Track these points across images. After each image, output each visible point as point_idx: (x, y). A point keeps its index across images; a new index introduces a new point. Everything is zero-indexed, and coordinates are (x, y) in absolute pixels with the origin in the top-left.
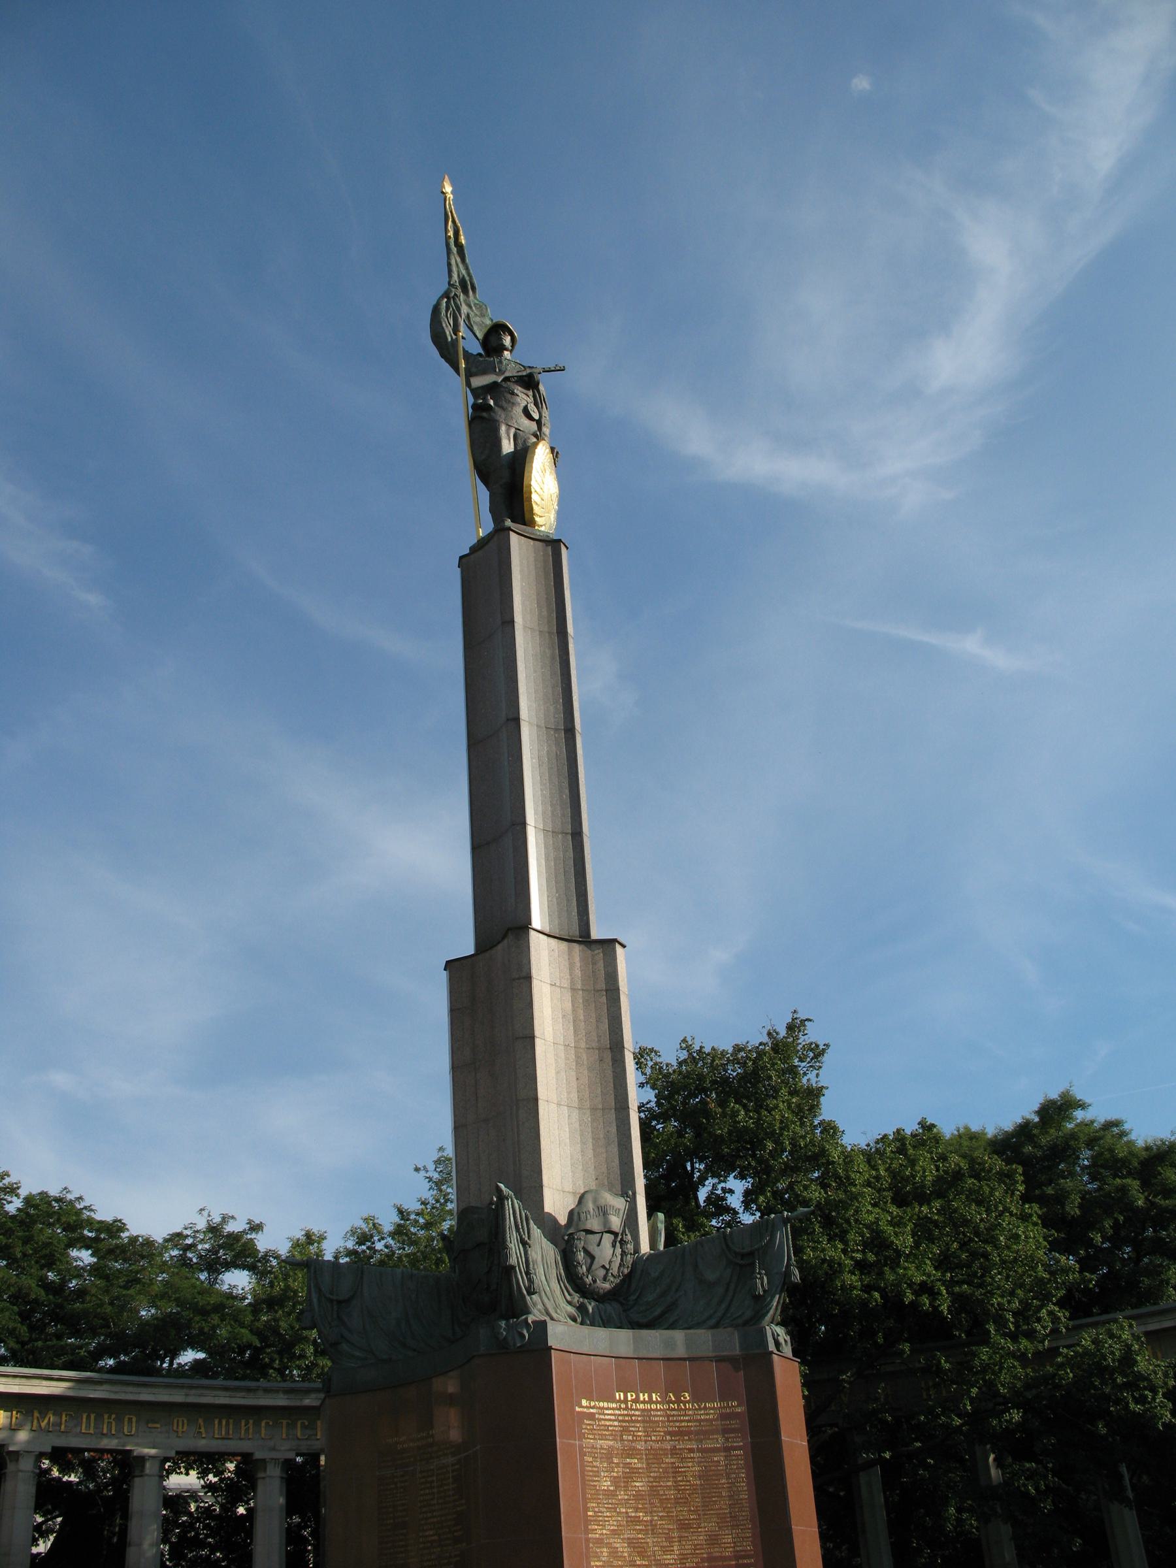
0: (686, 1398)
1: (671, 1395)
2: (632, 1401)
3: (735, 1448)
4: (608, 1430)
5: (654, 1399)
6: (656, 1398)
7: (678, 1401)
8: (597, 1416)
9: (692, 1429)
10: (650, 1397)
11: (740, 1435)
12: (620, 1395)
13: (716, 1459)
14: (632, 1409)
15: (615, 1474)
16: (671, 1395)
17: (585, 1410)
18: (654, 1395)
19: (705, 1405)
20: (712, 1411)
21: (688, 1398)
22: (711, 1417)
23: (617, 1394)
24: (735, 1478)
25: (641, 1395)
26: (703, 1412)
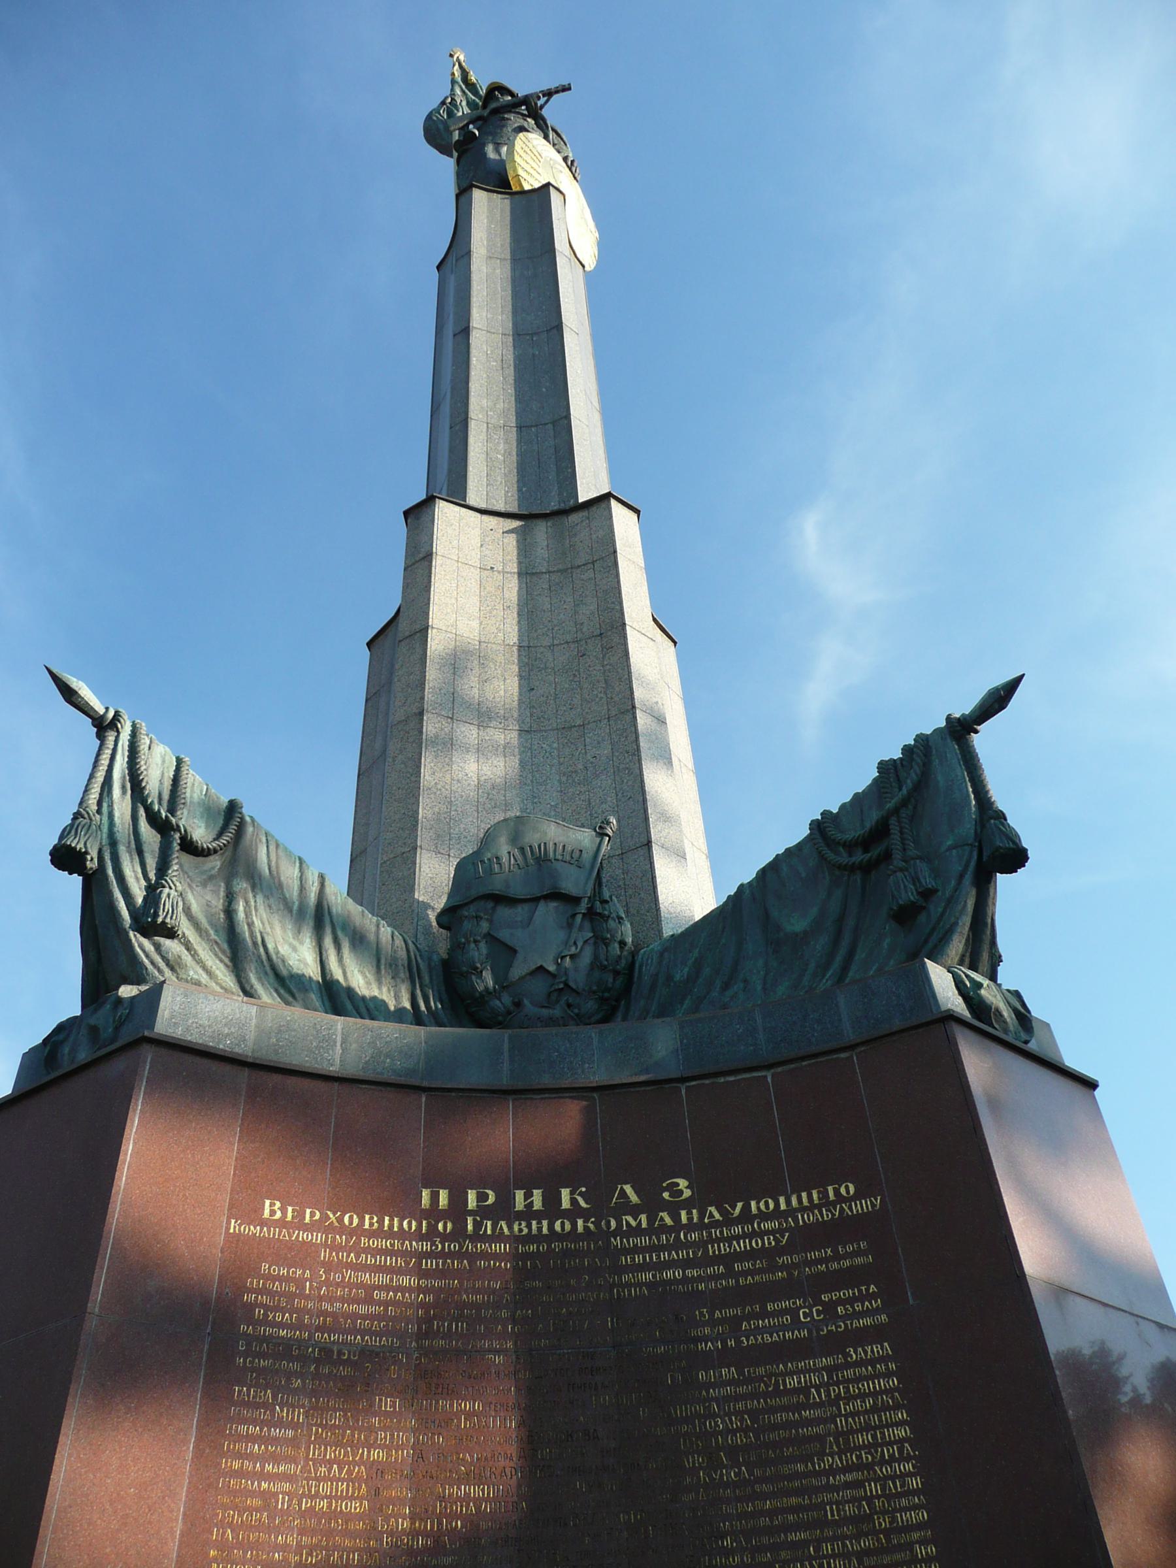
0: (681, 1192)
1: (628, 1189)
2: (483, 1212)
3: (861, 1337)
4: (369, 1300)
5: (566, 1203)
6: (574, 1202)
7: (651, 1205)
8: (323, 1255)
9: (702, 1287)
10: (552, 1200)
11: (873, 1288)
12: (435, 1197)
13: (792, 1382)
14: (477, 1237)
15: (377, 1454)
16: (628, 1189)
17: (275, 1232)
18: (565, 1193)
19: (747, 1207)
20: (768, 1225)
21: (687, 1193)
22: (769, 1241)
23: (426, 1194)
24: (868, 1447)
25: (519, 1195)
26: (738, 1230)
